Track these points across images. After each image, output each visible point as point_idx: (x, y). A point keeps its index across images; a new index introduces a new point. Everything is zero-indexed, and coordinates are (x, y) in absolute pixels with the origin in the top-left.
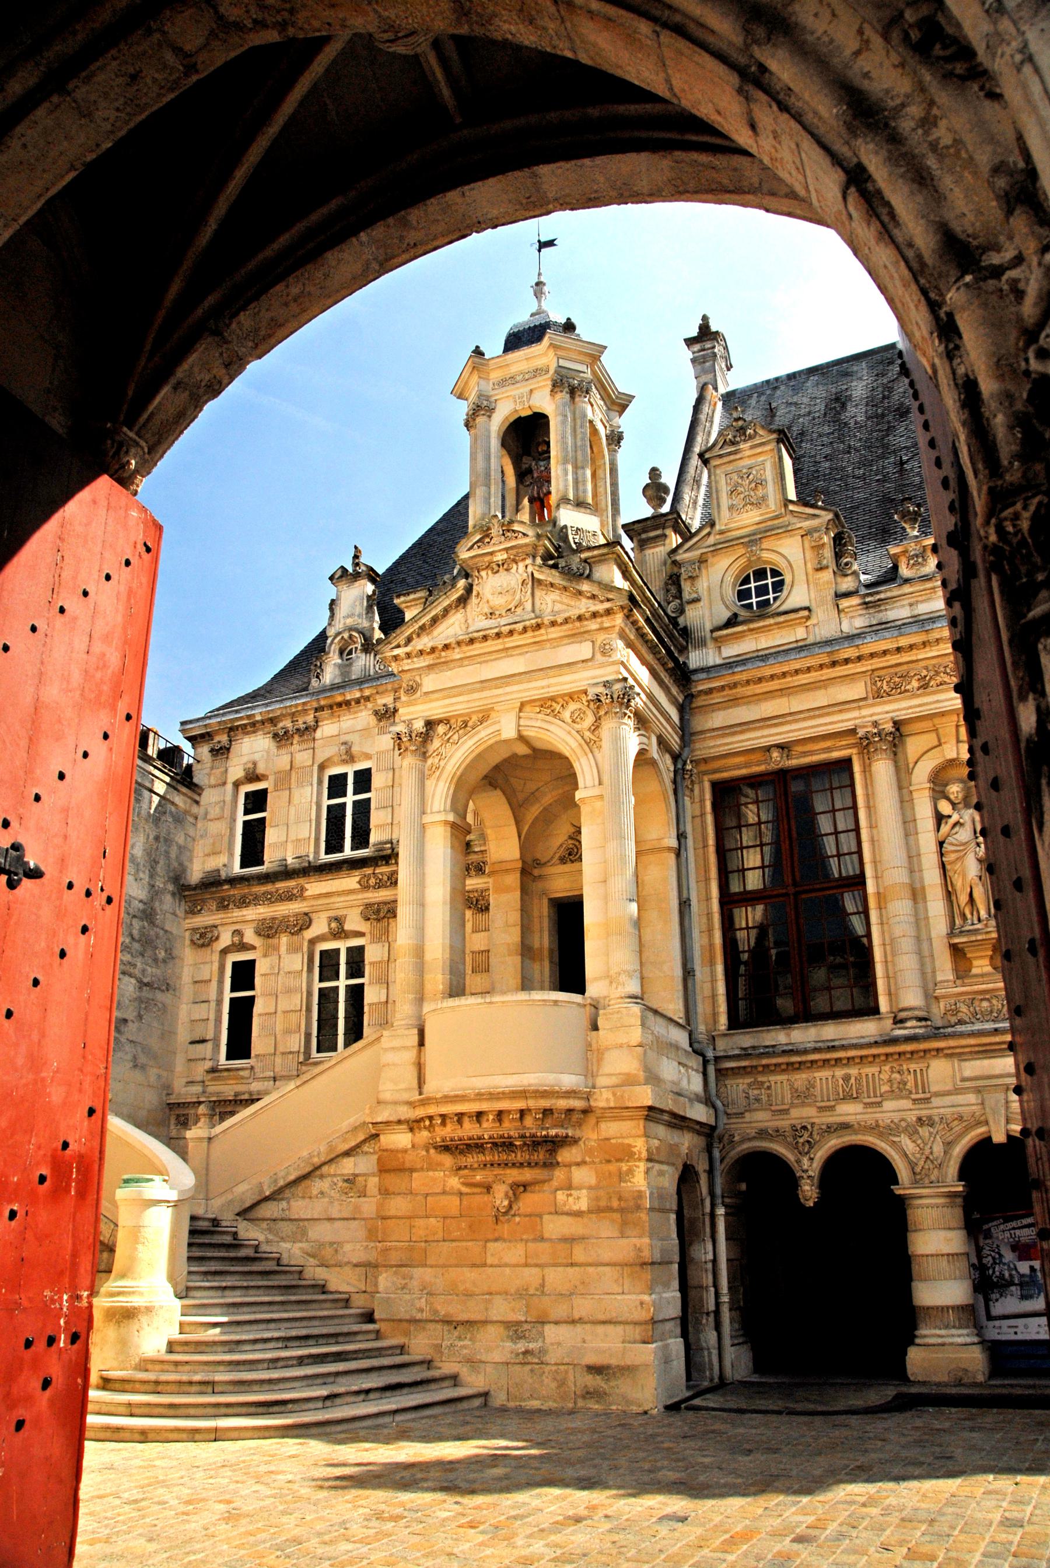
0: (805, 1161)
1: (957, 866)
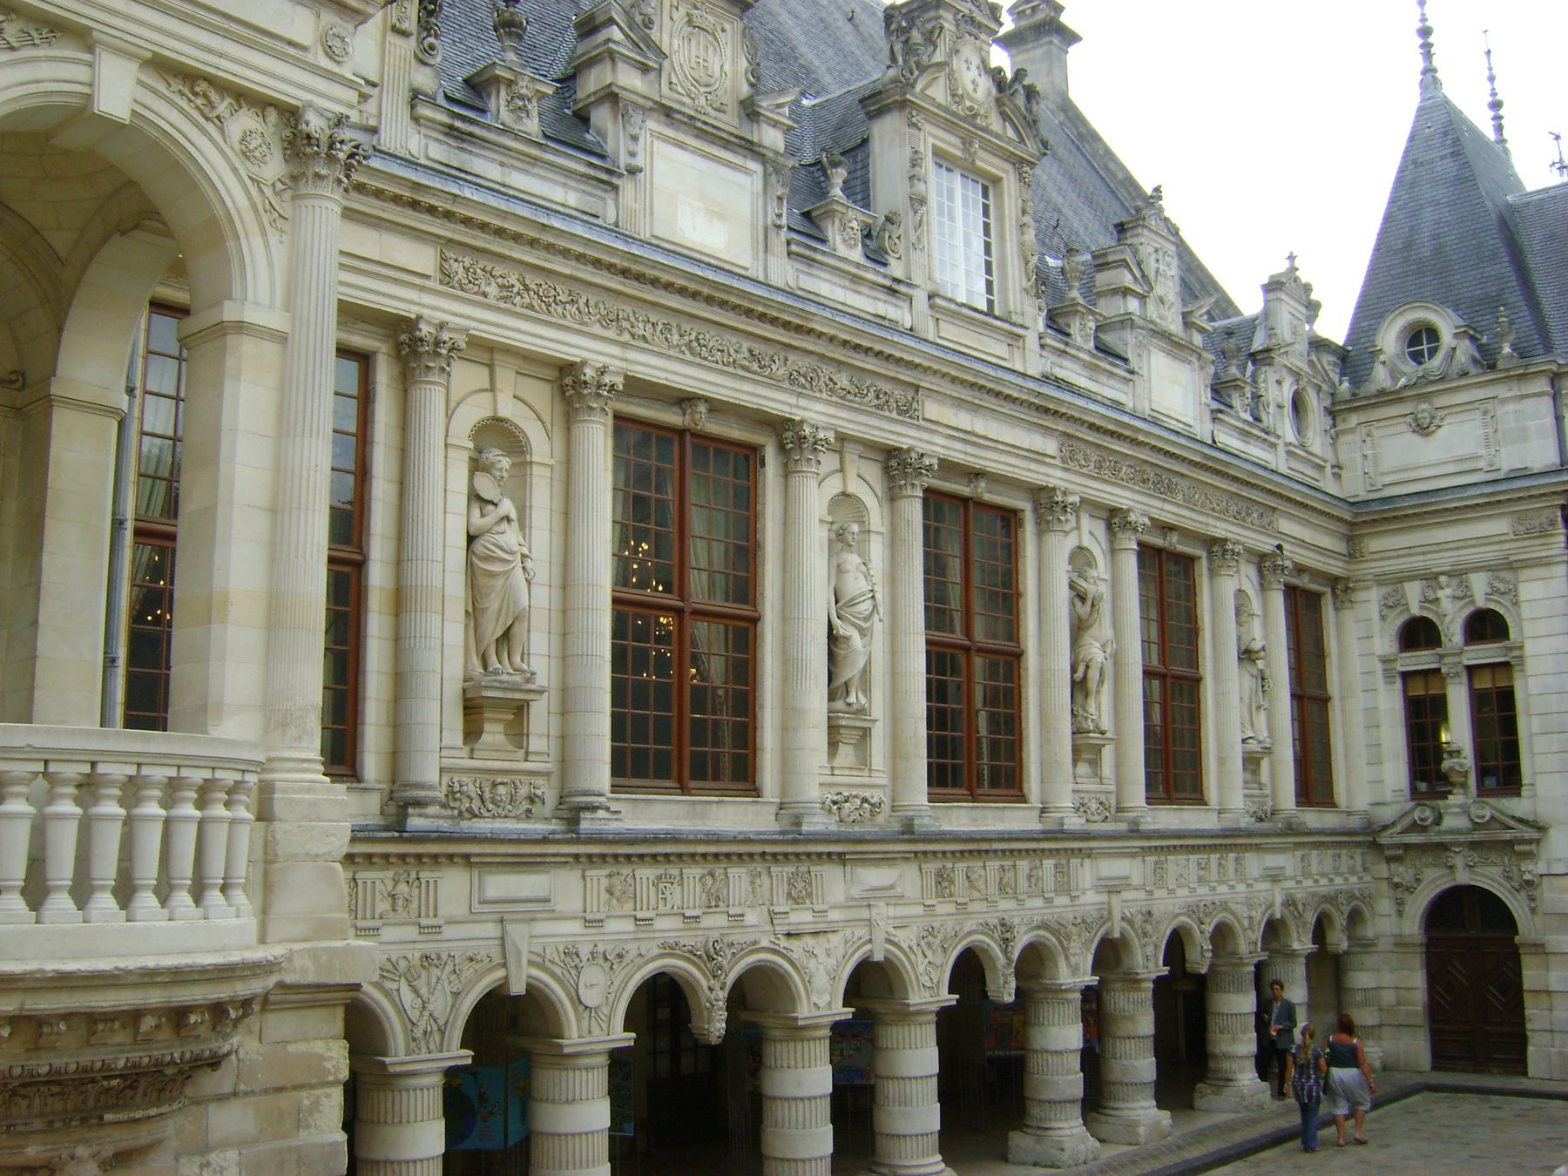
1: (499, 583)
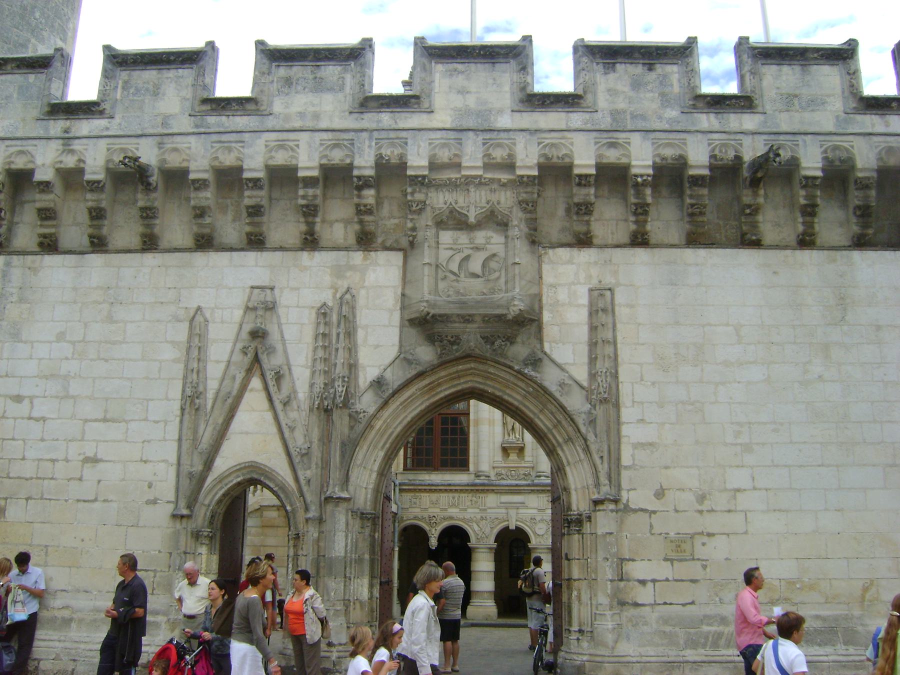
0: (433, 530)
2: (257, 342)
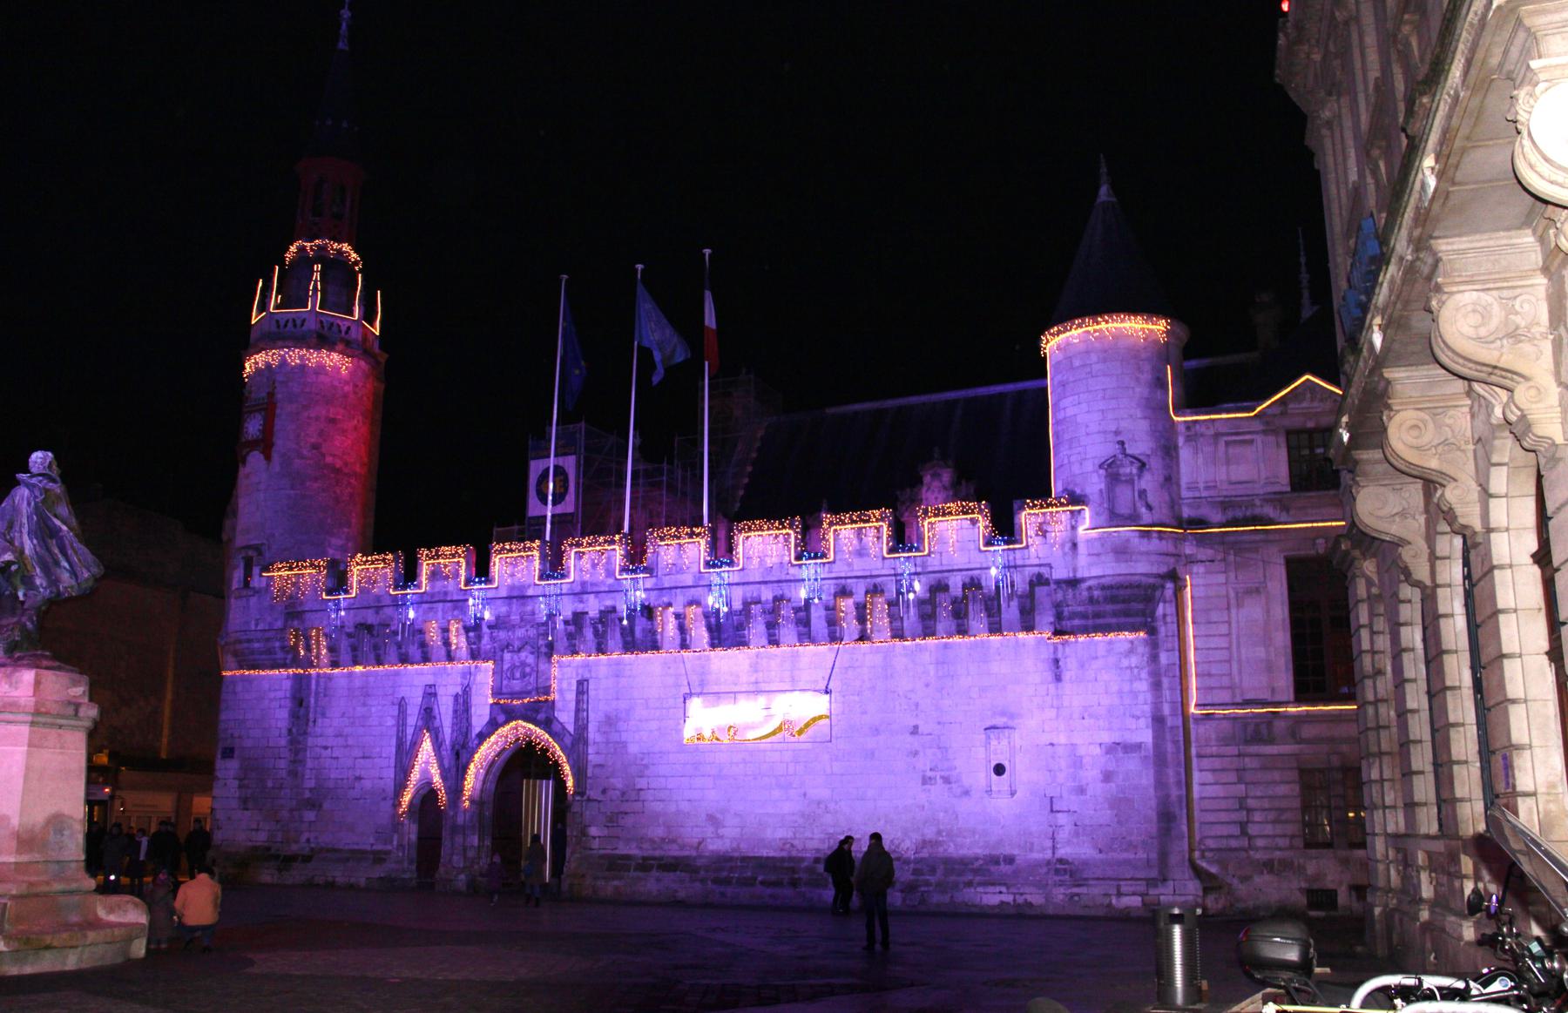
2: (428, 714)
